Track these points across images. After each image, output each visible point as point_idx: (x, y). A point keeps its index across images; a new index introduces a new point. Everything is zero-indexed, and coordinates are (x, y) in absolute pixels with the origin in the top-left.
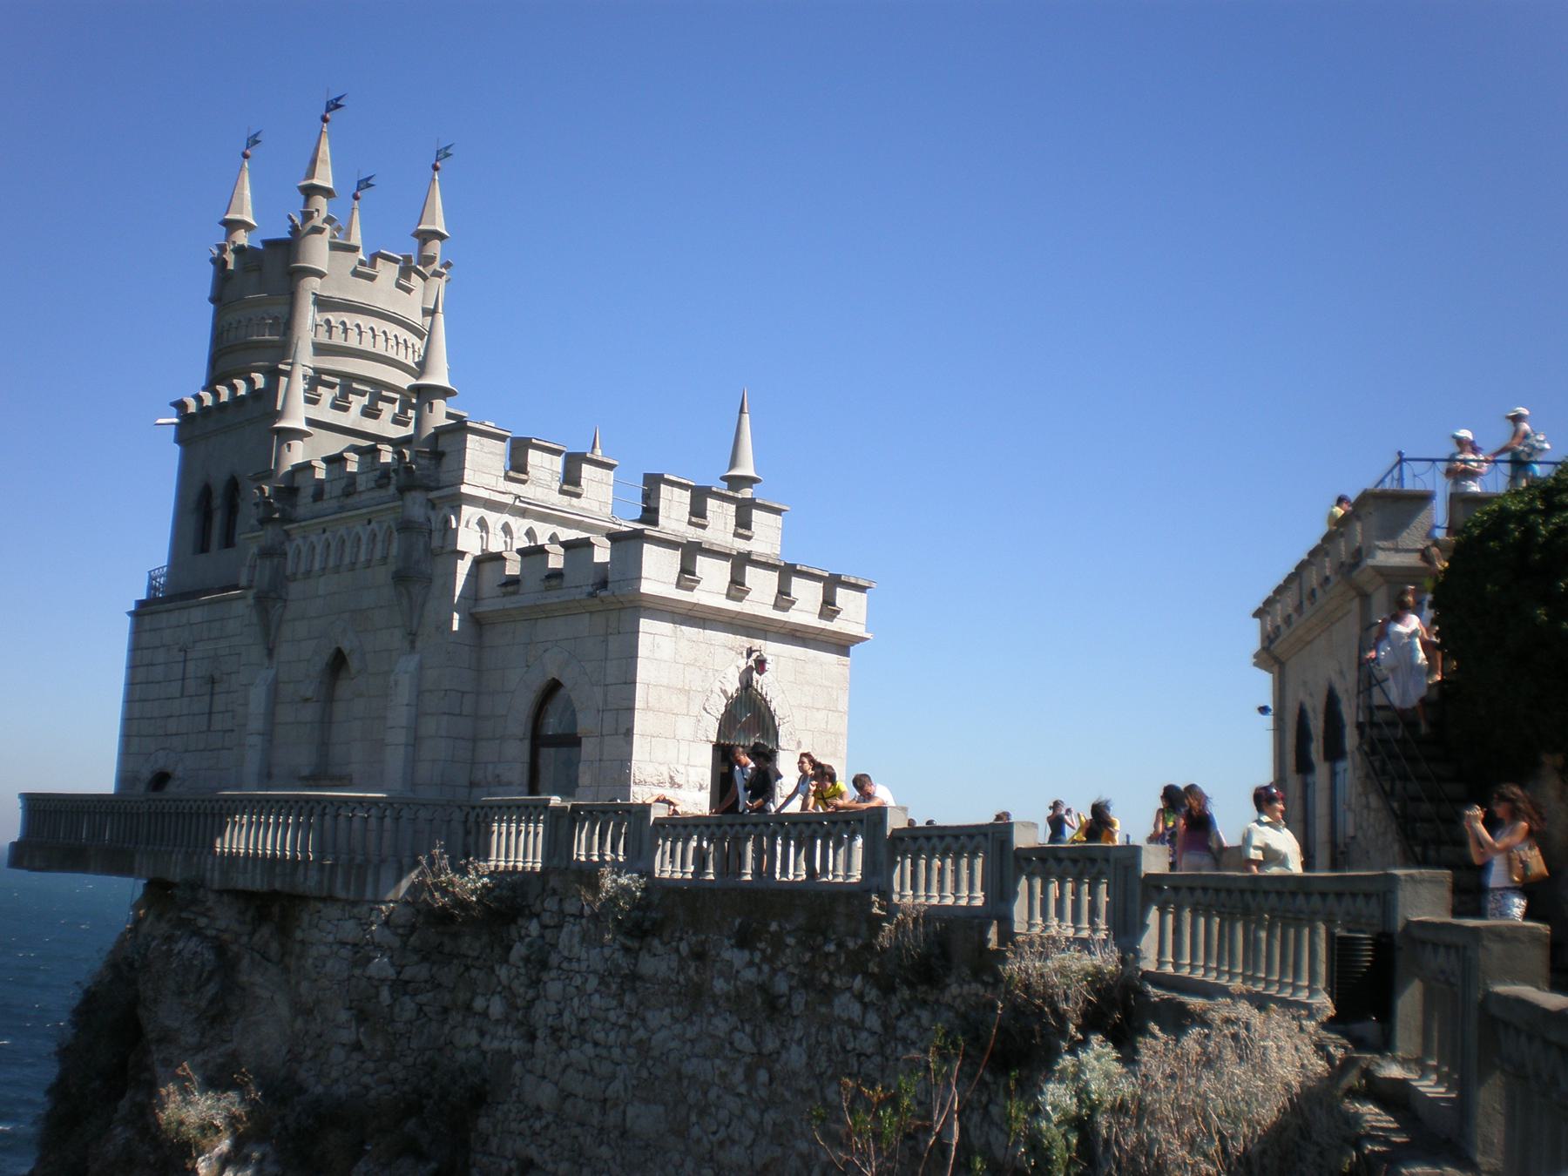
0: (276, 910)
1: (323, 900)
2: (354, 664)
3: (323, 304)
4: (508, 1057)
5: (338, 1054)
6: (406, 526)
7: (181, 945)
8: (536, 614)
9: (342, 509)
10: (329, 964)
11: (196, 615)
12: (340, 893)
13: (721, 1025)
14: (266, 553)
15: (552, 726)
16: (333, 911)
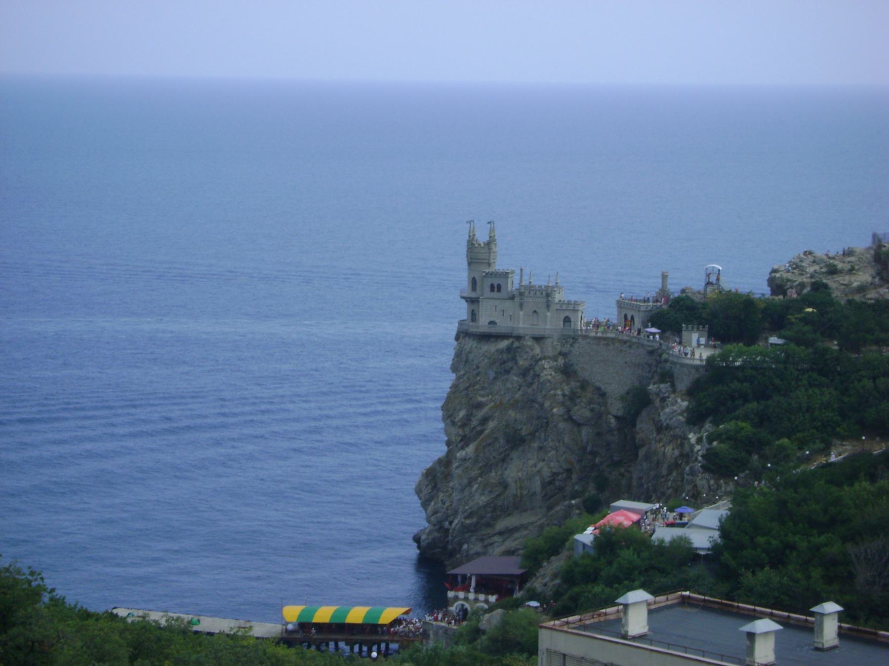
6: (548, 301)
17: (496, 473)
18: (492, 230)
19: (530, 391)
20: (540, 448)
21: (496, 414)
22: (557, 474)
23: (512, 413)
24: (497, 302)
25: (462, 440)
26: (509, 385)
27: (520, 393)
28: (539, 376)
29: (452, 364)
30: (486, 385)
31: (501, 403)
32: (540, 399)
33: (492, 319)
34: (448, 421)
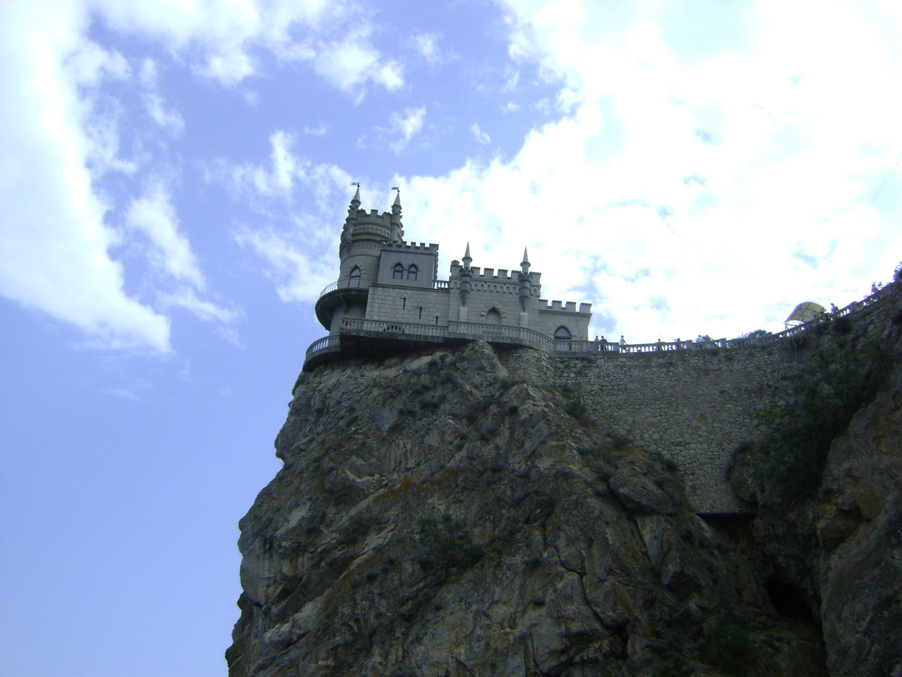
2: (501, 311)
4: (580, 383)
11: (408, 291)
13: (655, 369)
15: (559, 334)
16: (532, 351)
17: (385, 656)
18: (398, 199)
19: (487, 451)
20: (534, 565)
21: (393, 513)
22: (581, 639)
23: (438, 505)
24: (408, 293)
25: (285, 594)
26: (432, 440)
27: (459, 456)
28: (514, 411)
30: (372, 442)
31: (407, 485)
32: (517, 463)
34: (258, 544)
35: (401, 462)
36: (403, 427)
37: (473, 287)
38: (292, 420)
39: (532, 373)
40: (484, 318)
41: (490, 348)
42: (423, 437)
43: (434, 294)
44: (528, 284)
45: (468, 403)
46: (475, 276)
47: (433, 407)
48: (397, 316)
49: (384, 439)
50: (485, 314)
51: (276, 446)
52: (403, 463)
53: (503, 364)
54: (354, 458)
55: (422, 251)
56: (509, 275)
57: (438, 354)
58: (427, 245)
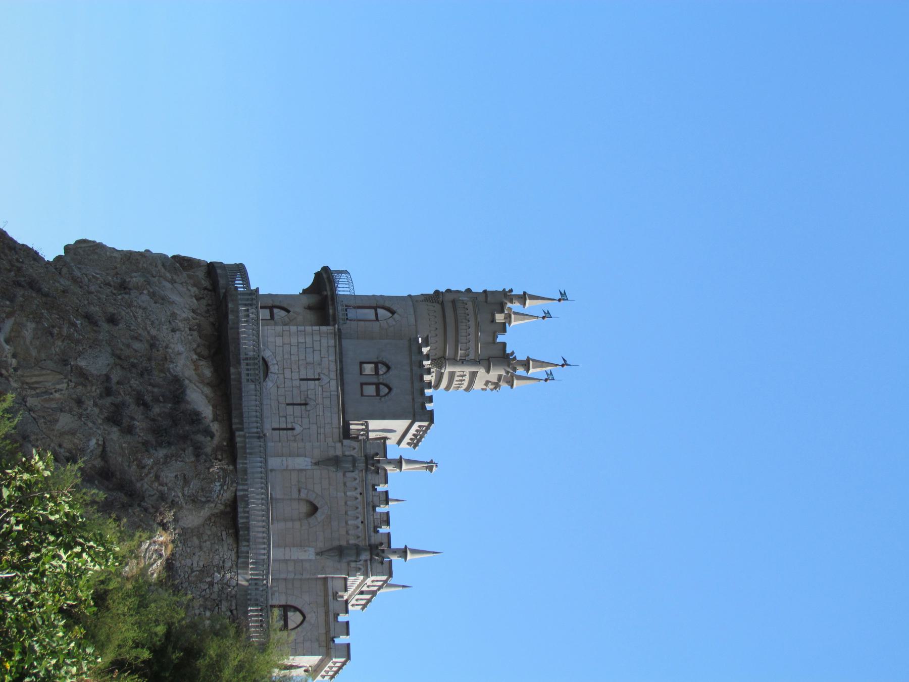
0: (228, 509)
1: (237, 552)
2: (312, 520)
3: (473, 375)
5: (188, 562)
6: (358, 550)
7: (218, 484)
8: (326, 605)
9: (368, 504)
10: (217, 557)
12: (240, 560)
14: (354, 461)
29: (100, 246)
33: (273, 369)
35: (35, 389)
36: (86, 386)
37: (349, 475)
38: (115, 255)
39: (196, 558)
40: (295, 495)
41: (227, 495)
42: (70, 411)
43: (335, 422)
44: (365, 556)
45: (126, 464)
46: (371, 478)
47: (114, 418)
48: (288, 372)
49: (65, 362)
50: (303, 495)
51: (78, 242)
52: (34, 392)
53: (209, 518)
54: (31, 326)
55: (419, 400)
56: (384, 530)
57: (215, 427)
58: (429, 406)
